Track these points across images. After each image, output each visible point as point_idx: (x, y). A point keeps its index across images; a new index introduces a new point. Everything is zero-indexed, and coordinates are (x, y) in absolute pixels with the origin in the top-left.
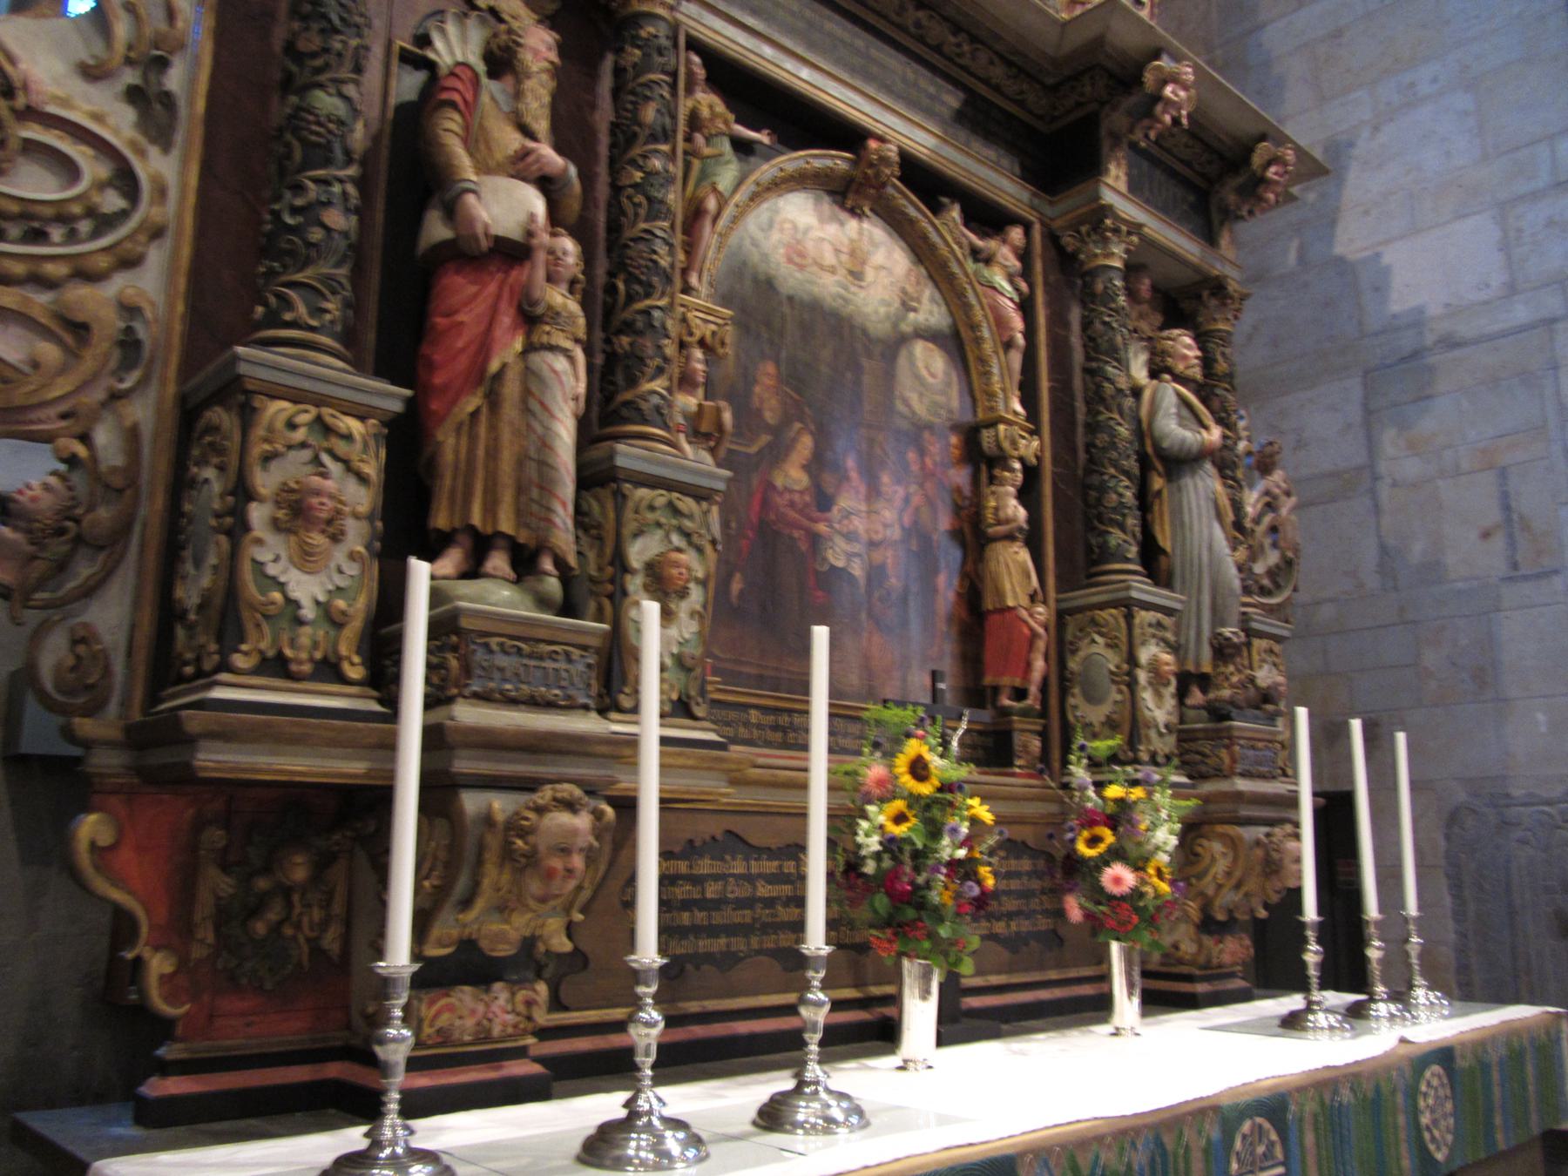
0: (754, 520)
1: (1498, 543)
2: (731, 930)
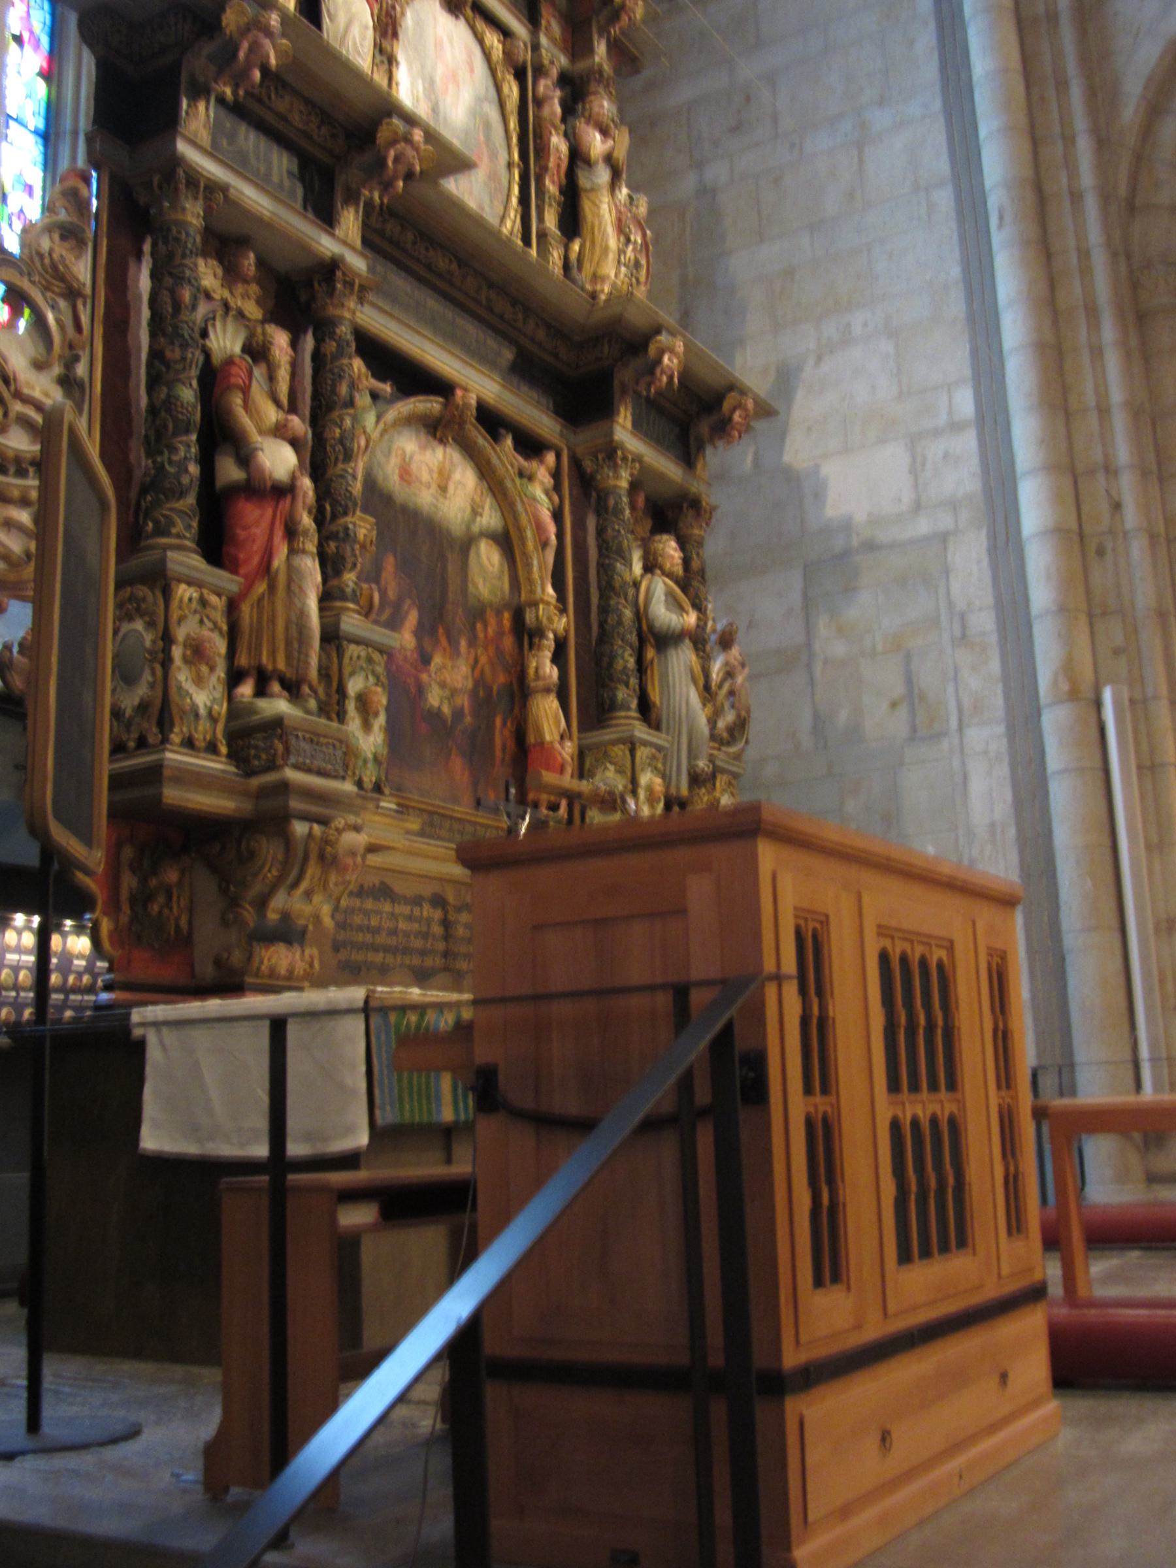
1: (903, 712)
2: (386, 949)
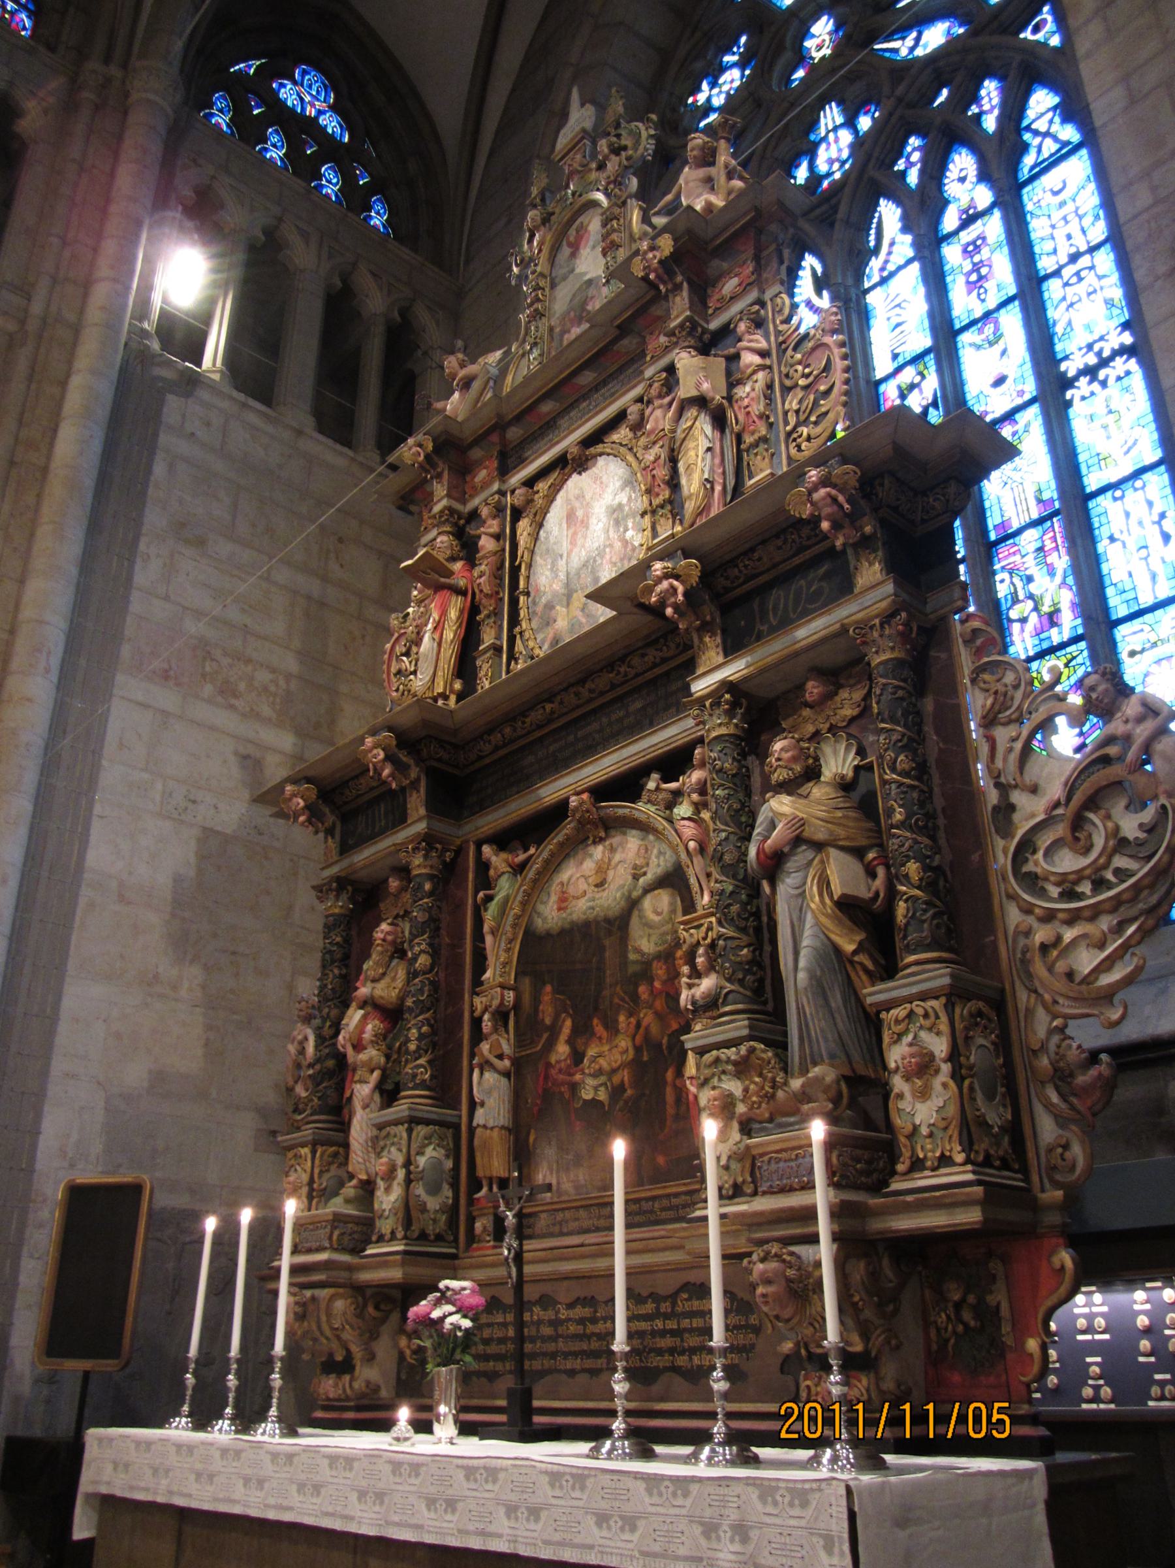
0: (540, 1091)
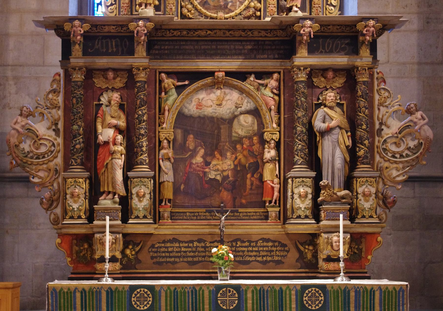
2: (175, 257)
